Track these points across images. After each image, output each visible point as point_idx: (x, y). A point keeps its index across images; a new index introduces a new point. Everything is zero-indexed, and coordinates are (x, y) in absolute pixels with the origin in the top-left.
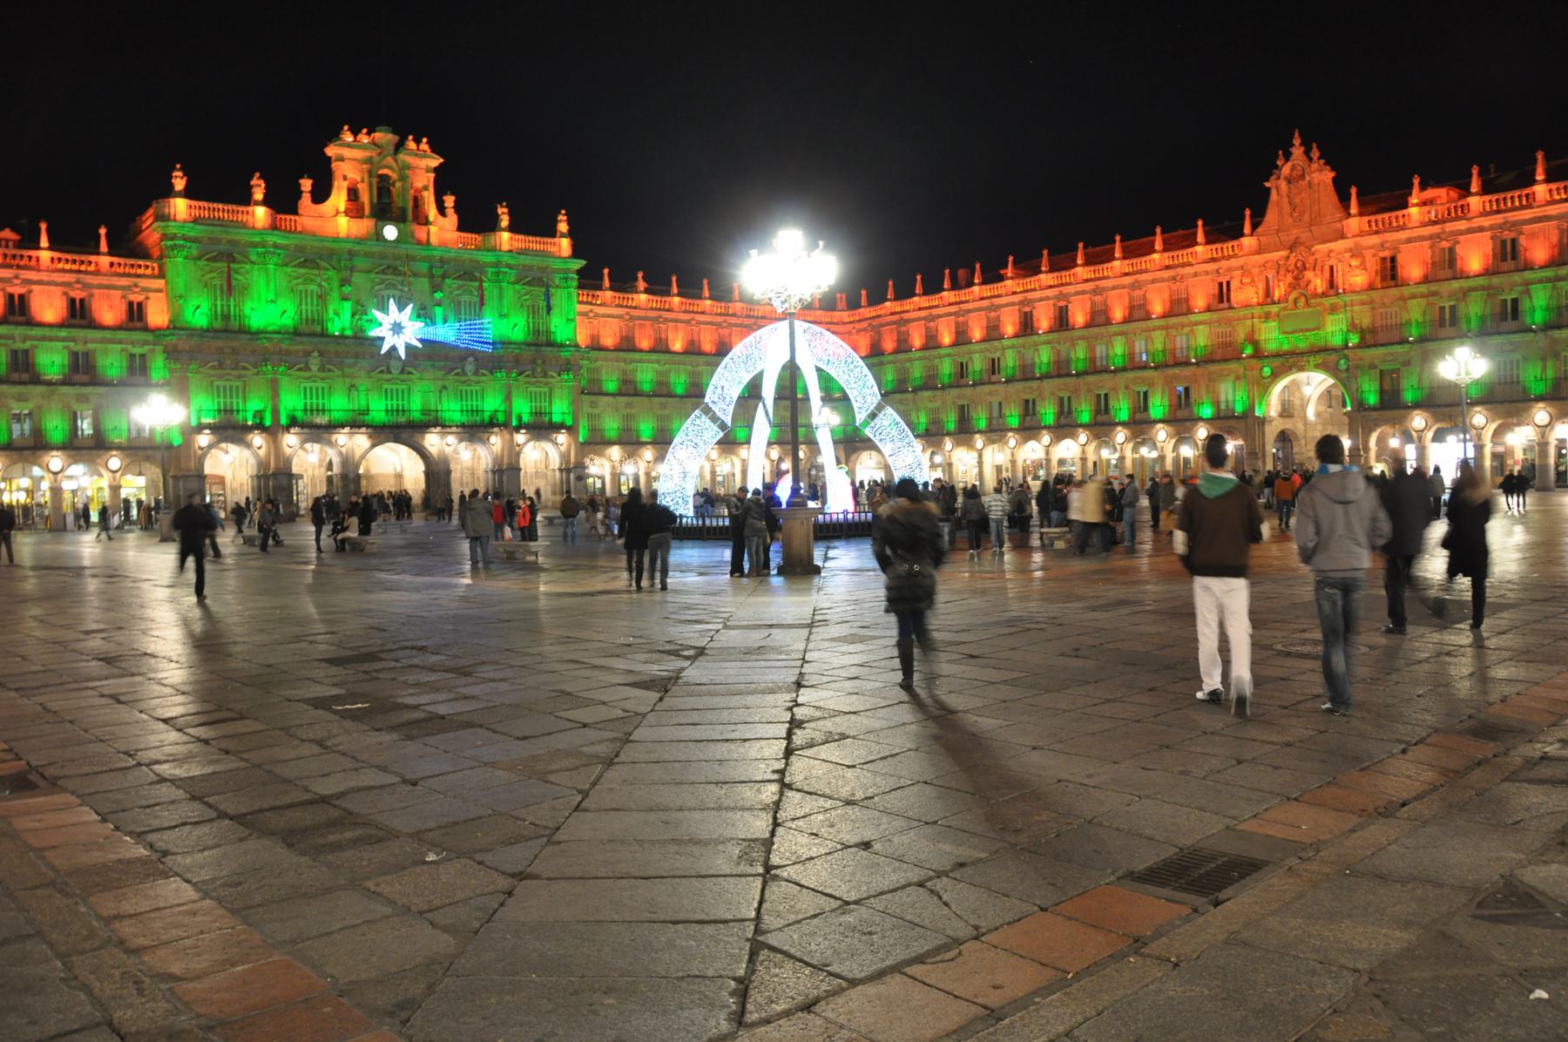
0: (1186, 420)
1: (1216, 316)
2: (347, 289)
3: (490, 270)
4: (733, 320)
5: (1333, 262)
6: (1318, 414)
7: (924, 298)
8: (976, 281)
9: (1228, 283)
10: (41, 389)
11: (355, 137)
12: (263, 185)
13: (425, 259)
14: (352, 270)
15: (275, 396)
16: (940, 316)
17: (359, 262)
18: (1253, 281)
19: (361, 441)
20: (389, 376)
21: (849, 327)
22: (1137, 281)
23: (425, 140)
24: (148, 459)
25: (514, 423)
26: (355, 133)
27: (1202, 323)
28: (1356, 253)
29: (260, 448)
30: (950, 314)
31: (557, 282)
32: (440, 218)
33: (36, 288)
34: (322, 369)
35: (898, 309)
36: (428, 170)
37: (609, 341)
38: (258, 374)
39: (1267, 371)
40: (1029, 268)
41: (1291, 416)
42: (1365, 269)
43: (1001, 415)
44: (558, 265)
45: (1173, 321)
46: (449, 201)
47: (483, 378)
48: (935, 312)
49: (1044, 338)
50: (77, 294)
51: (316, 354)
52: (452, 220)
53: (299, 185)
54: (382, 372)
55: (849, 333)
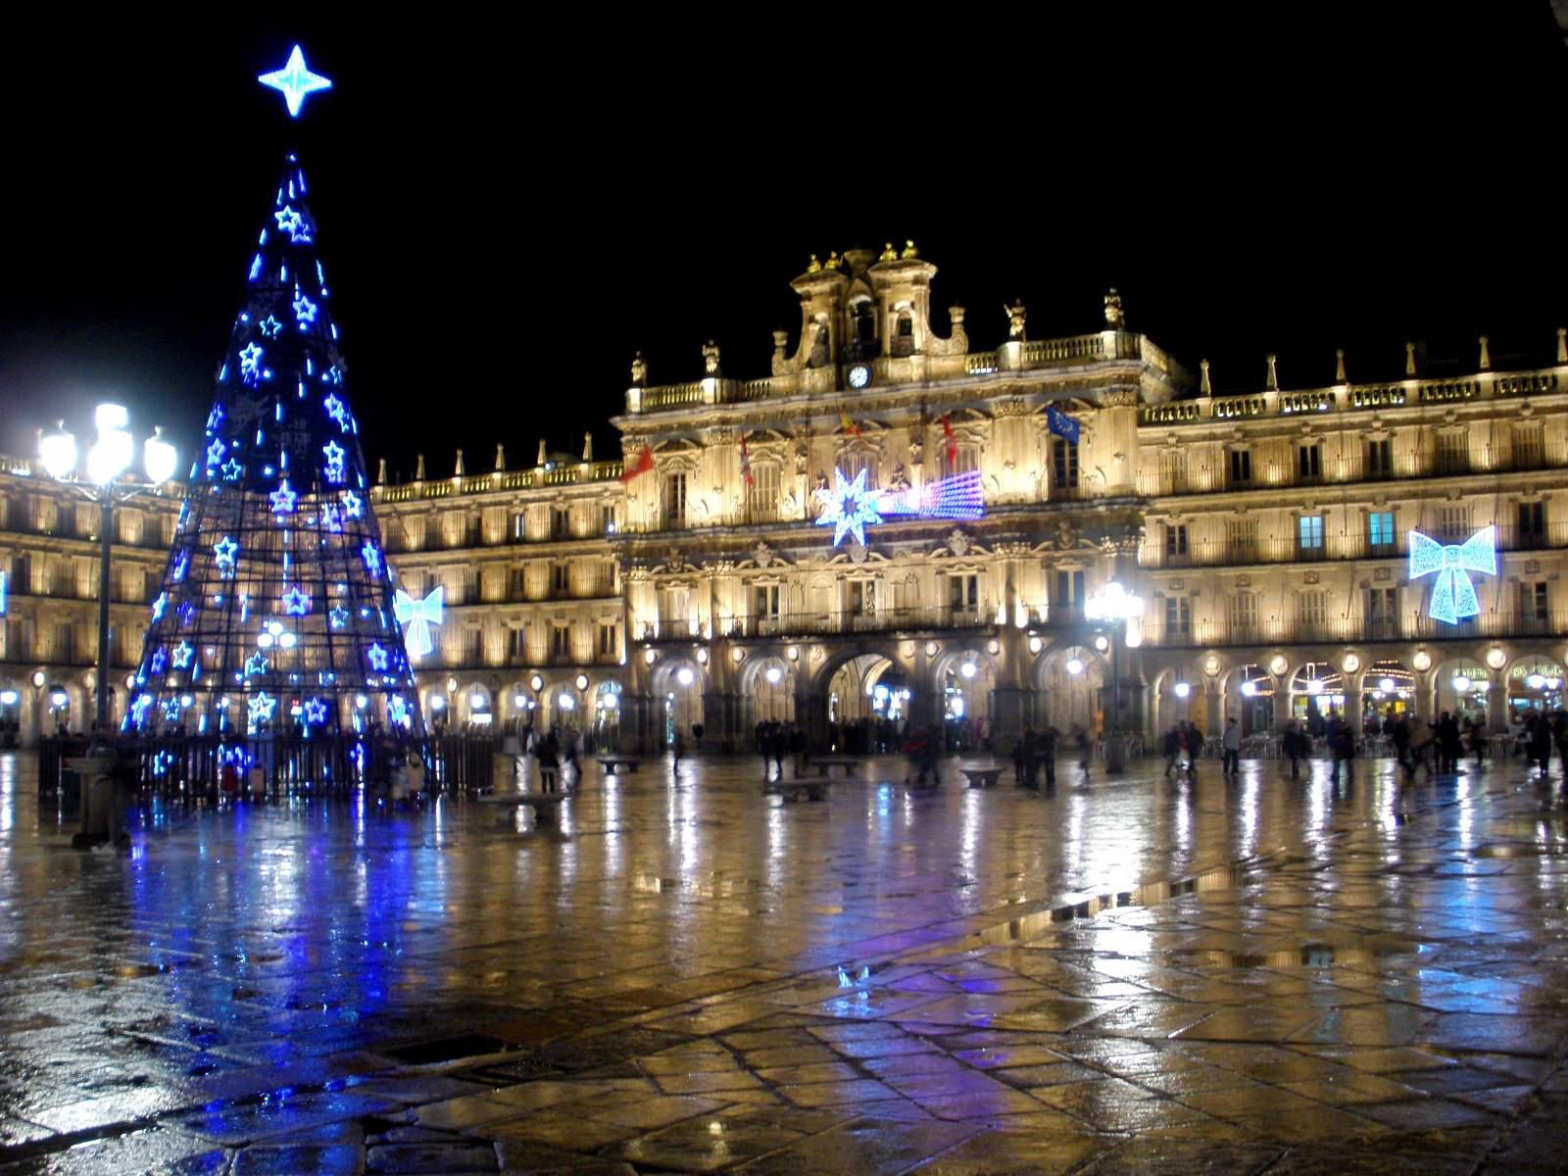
2: (800, 460)
3: (992, 400)
10: (526, 608)
11: (823, 266)
12: (717, 353)
13: (898, 403)
14: (813, 433)
15: (714, 599)
17: (819, 423)
19: (817, 656)
20: (850, 567)
23: (910, 244)
24: (612, 677)
25: (1021, 621)
26: (823, 260)
29: (705, 664)
31: (1100, 400)
32: (938, 344)
33: (531, 506)
34: (770, 565)
36: (917, 281)
37: (1204, 481)
38: (704, 576)
44: (1096, 373)
46: (957, 316)
47: (979, 558)
50: (561, 507)
51: (761, 547)
52: (958, 340)
53: (773, 339)
54: (840, 562)
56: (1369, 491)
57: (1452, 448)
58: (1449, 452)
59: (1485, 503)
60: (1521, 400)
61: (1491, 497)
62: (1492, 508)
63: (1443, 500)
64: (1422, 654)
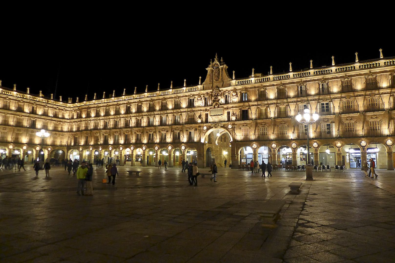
0: (178, 143)
1: (189, 110)
4: (25, 100)
5: (227, 94)
6: (218, 143)
7: (96, 101)
8: (113, 96)
9: (193, 100)
16: (101, 107)
18: (201, 99)
21: (72, 109)
22: (164, 97)
27: (184, 112)
28: (235, 90)
30: (104, 106)
35: (88, 104)
39: (205, 128)
40: (129, 93)
41: (211, 143)
42: (237, 96)
43: (118, 140)
45: (175, 111)
48: (99, 105)
49: (133, 115)
55: (72, 111)
56: (4, 111)
57: (21, 107)
58: (20, 107)
59: (26, 118)
60: (34, 102)
61: (27, 118)
62: (27, 120)
63: (18, 116)
64: (11, 146)
